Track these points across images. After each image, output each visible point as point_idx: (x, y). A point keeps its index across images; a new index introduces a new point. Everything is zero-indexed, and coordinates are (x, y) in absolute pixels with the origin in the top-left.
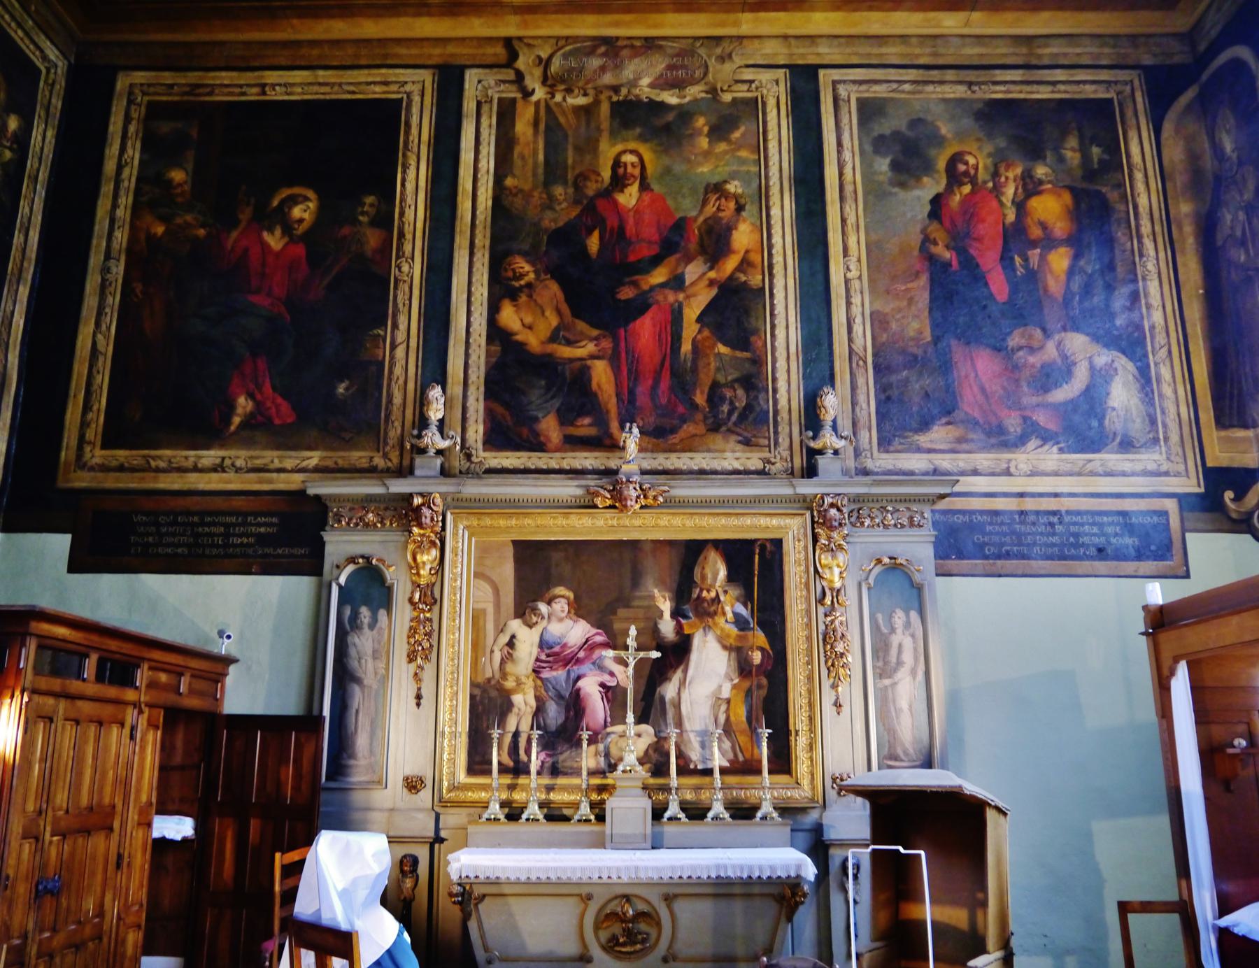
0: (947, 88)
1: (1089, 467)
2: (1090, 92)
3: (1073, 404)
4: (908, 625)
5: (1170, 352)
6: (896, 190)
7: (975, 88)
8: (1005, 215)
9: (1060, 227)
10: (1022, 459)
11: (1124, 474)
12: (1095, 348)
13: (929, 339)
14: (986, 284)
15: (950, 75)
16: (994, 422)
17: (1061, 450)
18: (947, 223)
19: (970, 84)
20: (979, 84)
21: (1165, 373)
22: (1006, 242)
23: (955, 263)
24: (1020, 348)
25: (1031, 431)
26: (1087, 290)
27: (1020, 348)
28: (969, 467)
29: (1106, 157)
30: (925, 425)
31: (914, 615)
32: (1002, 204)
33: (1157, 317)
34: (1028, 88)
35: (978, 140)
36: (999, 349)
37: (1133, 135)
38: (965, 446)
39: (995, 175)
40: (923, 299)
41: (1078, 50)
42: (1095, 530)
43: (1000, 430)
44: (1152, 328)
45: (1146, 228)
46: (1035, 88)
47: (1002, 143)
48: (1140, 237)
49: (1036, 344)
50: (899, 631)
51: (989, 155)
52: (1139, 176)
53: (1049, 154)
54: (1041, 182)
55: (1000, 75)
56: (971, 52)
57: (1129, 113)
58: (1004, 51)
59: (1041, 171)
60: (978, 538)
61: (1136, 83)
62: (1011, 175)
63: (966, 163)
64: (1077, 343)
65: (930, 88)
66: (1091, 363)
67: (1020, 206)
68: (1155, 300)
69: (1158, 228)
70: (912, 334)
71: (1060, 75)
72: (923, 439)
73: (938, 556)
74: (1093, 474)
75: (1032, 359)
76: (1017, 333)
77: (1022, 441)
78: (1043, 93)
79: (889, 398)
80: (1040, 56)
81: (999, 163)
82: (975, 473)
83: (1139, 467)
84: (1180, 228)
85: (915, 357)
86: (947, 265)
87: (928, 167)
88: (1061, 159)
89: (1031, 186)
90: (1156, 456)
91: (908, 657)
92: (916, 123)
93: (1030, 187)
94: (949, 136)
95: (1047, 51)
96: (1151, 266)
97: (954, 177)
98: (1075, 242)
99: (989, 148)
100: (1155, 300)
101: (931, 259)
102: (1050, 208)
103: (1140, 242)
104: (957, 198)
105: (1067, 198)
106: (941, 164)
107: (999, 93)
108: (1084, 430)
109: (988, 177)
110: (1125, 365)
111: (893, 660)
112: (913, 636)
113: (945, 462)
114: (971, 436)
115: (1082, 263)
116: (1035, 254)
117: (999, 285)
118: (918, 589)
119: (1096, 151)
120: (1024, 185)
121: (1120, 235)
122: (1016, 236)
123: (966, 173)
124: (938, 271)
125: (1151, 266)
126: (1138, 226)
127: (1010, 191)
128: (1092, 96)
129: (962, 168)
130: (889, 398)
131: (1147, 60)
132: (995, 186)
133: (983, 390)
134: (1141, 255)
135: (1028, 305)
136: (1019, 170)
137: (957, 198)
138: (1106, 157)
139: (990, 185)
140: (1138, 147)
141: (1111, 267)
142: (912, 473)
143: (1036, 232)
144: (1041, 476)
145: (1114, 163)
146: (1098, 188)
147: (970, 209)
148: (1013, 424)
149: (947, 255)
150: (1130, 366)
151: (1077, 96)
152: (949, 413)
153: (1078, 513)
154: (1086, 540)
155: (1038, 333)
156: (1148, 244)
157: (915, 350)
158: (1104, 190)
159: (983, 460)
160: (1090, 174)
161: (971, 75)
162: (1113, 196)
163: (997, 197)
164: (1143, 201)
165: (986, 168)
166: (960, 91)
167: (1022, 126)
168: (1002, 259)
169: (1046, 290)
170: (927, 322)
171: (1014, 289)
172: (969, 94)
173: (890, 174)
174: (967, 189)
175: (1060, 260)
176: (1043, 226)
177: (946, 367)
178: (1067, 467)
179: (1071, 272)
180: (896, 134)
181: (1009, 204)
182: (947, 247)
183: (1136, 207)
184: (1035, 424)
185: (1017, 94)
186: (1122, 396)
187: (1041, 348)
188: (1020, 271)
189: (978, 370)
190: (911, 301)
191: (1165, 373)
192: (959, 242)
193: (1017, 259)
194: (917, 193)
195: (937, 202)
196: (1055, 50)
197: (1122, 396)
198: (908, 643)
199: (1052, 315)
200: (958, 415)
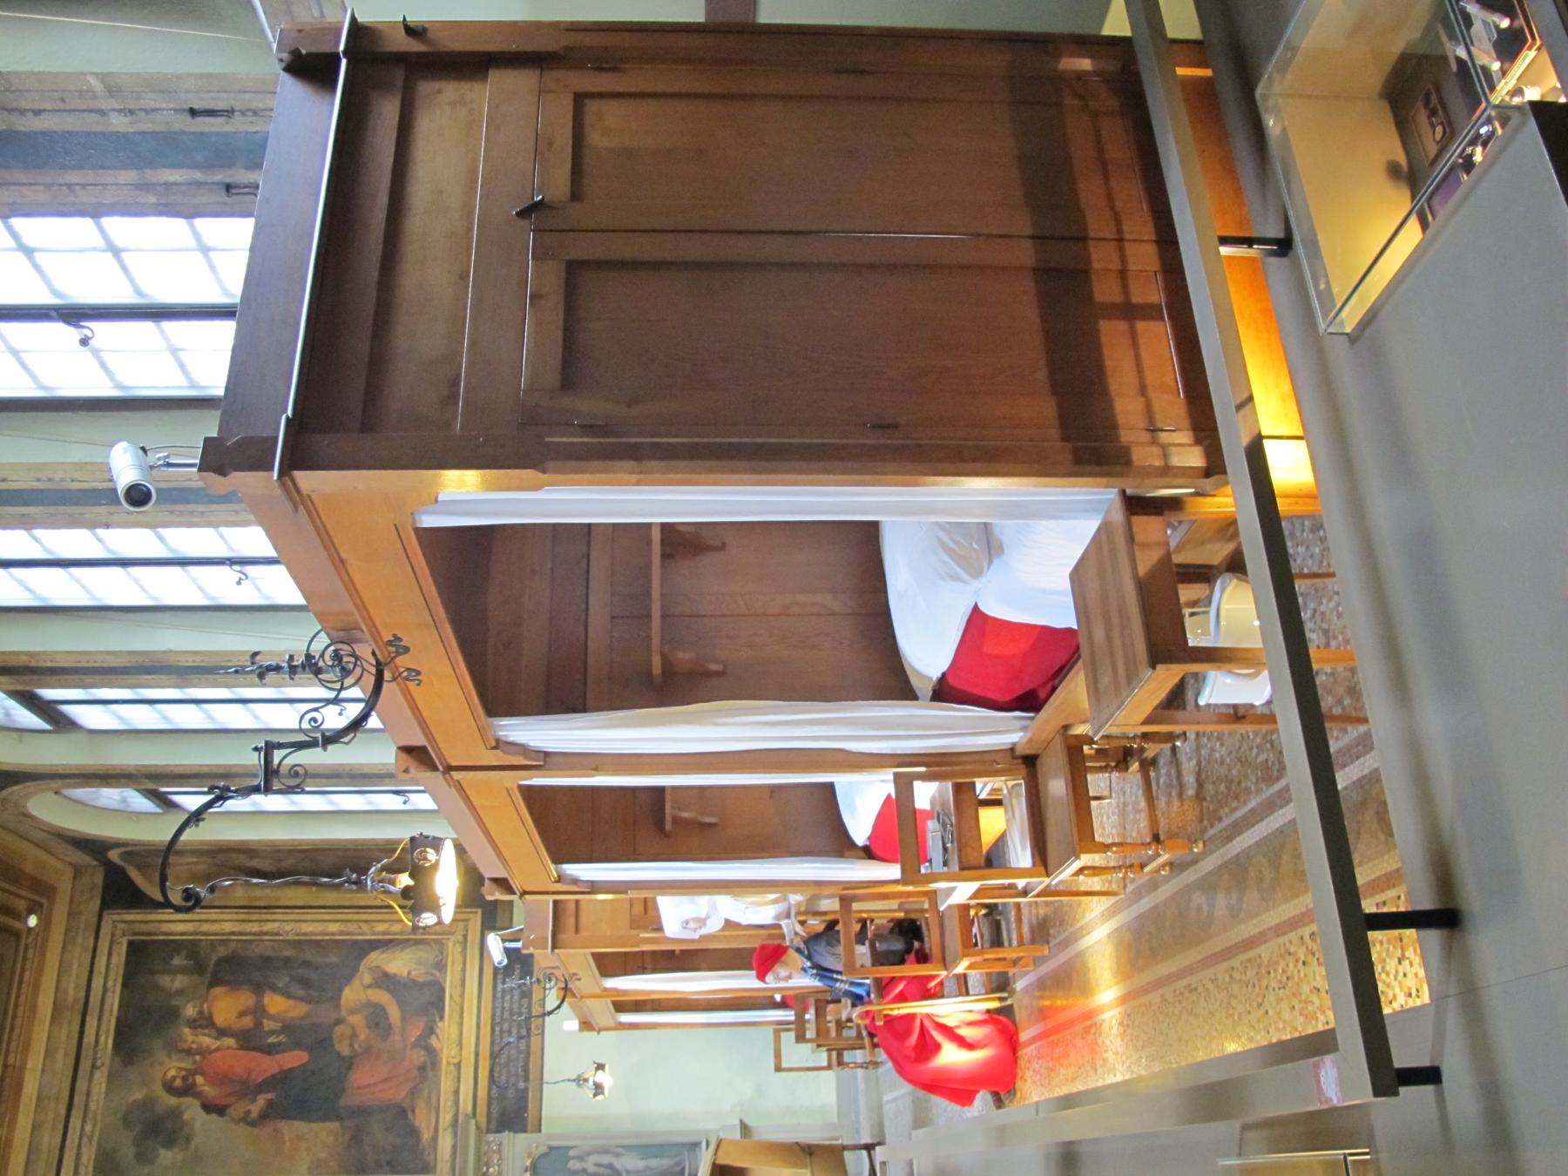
0: (95, 1091)
1: (456, 997)
2: (120, 957)
3: (401, 1004)
4: (580, 1158)
5: (366, 921)
6: (193, 1145)
7: (99, 1063)
8: (229, 1048)
9: (246, 999)
10: (447, 1053)
11: (464, 970)
12: (356, 983)
13: (336, 1124)
14: (292, 1069)
15: (81, 1085)
16: (415, 1073)
17: (442, 1018)
18: (230, 1100)
19: (94, 1067)
20: (95, 1059)
21: (381, 927)
22: (254, 1049)
23: (270, 1096)
24: (351, 1045)
25: (424, 1043)
26: (305, 983)
27: (351, 1045)
28: (452, 1098)
29: (184, 953)
30: (414, 1133)
31: (571, 1153)
32: (217, 1050)
33: (333, 928)
34: (106, 1013)
35: (152, 1065)
36: (349, 1063)
37: (166, 927)
38: (434, 1100)
39: (189, 1052)
40: (300, 1127)
41: (75, 966)
42: (508, 998)
43: (422, 1068)
44: (342, 933)
45: (255, 928)
46: (107, 1008)
47: (157, 1044)
48: (262, 933)
49: (348, 1032)
50: (584, 1165)
51: (169, 1056)
52: (205, 927)
53: (174, 1002)
54: (201, 1013)
55: (90, 1036)
56: (63, 1062)
57: (144, 928)
58: (64, 1032)
59: (190, 1011)
60: (511, 1093)
61: (116, 917)
62: (190, 1038)
63: (174, 1078)
64: (352, 994)
65: (93, 1106)
66: (369, 986)
67: (222, 1033)
68: (319, 927)
69: (254, 917)
70: (331, 1139)
71: (97, 984)
72: (426, 1136)
73: (525, 1131)
74: (462, 995)
75: (362, 1037)
76: (337, 1047)
77: (432, 1053)
78: (114, 1001)
79: (389, 1163)
80: (76, 1001)
81: (175, 1048)
82: (457, 1092)
83: (459, 958)
84: (256, 899)
85: (353, 1138)
86: (270, 1103)
87: (175, 1114)
88: (180, 992)
89: (203, 1022)
90: (451, 944)
91: (605, 1159)
92: (127, 1121)
93: (204, 1022)
94: (145, 1091)
95: (71, 992)
96: (288, 927)
97: (188, 1090)
98: (258, 988)
99: (162, 1056)
100: (319, 927)
101: (264, 1116)
102: (227, 1006)
103: (266, 934)
104: (207, 1088)
105: (218, 990)
106: (173, 1101)
107: (108, 1041)
108: (428, 1000)
109: (190, 1060)
110: (374, 958)
111: (607, 1171)
112: (589, 1154)
113: (446, 1118)
114: (425, 1092)
115: (280, 985)
116: (268, 1025)
117: (295, 1059)
118: (551, 1148)
119: (177, 961)
120: (201, 1027)
121: (257, 950)
122: (249, 1040)
123: (184, 1079)
124: (272, 1113)
125: (288, 927)
126: (250, 934)
127: (207, 1041)
128: (123, 959)
129: (178, 1082)
130: (389, 1163)
131: (96, 905)
132: (200, 1053)
133: (385, 1081)
134: (278, 934)
135: (315, 1039)
136: (187, 1030)
137: (207, 1088)
138: (184, 953)
139: (198, 1058)
140: (177, 925)
141: (287, 962)
142: (454, 1147)
143: (247, 1022)
144: (463, 1035)
145: (191, 948)
146: (211, 964)
147: (220, 1079)
148: (418, 1057)
149: (261, 1101)
150: (373, 955)
151: (121, 971)
152: (404, 1111)
153: (494, 1009)
154: (515, 1006)
155: (338, 1030)
156: (268, 927)
157: (347, 1137)
158: (214, 958)
159: (446, 1085)
160: (199, 968)
161: (85, 1065)
162: (221, 952)
163: (211, 1052)
164: (228, 927)
165: (179, 1060)
166: (100, 1078)
167: (142, 1024)
168: (269, 1053)
169: (302, 1018)
170: (321, 1125)
171: (297, 1045)
172: (105, 1070)
173: (176, 1150)
174: (199, 1079)
175: (275, 1004)
176: (242, 1014)
177: (363, 1111)
178: (456, 1018)
179: (288, 995)
180: (138, 1141)
181: (218, 1043)
182: (254, 1101)
183: (233, 933)
184: (419, 1039)
185: (110, 1024)
186: (400, 964)
187: (353, 1027)
188: (282, 1038)
189: (368, 1084)
190: (300, 1138)
191: (381, 927)
192: (248, 1090)
193: (271, 1040)
194: (198, 1126)
195: (208, 1108)
196: (72, 985)
197: (400, 964)
198: (593, 1159)
199: (324, 1014)
200: (406, 1104)
